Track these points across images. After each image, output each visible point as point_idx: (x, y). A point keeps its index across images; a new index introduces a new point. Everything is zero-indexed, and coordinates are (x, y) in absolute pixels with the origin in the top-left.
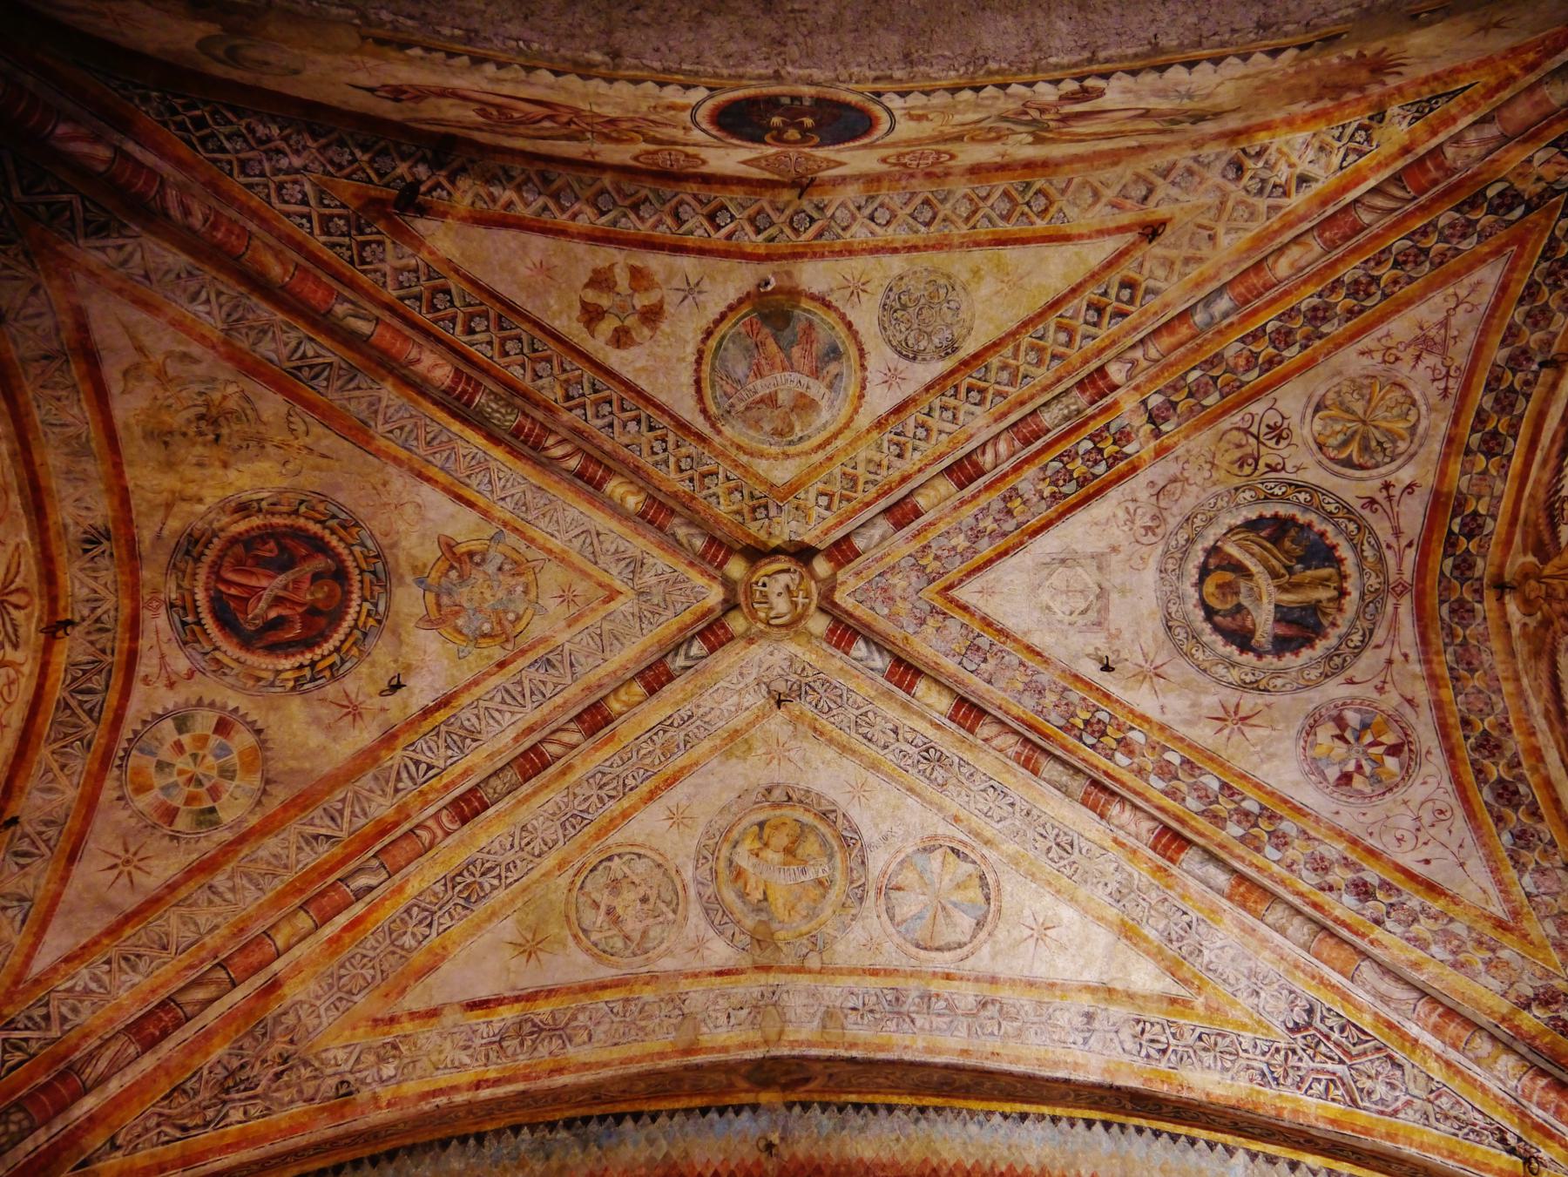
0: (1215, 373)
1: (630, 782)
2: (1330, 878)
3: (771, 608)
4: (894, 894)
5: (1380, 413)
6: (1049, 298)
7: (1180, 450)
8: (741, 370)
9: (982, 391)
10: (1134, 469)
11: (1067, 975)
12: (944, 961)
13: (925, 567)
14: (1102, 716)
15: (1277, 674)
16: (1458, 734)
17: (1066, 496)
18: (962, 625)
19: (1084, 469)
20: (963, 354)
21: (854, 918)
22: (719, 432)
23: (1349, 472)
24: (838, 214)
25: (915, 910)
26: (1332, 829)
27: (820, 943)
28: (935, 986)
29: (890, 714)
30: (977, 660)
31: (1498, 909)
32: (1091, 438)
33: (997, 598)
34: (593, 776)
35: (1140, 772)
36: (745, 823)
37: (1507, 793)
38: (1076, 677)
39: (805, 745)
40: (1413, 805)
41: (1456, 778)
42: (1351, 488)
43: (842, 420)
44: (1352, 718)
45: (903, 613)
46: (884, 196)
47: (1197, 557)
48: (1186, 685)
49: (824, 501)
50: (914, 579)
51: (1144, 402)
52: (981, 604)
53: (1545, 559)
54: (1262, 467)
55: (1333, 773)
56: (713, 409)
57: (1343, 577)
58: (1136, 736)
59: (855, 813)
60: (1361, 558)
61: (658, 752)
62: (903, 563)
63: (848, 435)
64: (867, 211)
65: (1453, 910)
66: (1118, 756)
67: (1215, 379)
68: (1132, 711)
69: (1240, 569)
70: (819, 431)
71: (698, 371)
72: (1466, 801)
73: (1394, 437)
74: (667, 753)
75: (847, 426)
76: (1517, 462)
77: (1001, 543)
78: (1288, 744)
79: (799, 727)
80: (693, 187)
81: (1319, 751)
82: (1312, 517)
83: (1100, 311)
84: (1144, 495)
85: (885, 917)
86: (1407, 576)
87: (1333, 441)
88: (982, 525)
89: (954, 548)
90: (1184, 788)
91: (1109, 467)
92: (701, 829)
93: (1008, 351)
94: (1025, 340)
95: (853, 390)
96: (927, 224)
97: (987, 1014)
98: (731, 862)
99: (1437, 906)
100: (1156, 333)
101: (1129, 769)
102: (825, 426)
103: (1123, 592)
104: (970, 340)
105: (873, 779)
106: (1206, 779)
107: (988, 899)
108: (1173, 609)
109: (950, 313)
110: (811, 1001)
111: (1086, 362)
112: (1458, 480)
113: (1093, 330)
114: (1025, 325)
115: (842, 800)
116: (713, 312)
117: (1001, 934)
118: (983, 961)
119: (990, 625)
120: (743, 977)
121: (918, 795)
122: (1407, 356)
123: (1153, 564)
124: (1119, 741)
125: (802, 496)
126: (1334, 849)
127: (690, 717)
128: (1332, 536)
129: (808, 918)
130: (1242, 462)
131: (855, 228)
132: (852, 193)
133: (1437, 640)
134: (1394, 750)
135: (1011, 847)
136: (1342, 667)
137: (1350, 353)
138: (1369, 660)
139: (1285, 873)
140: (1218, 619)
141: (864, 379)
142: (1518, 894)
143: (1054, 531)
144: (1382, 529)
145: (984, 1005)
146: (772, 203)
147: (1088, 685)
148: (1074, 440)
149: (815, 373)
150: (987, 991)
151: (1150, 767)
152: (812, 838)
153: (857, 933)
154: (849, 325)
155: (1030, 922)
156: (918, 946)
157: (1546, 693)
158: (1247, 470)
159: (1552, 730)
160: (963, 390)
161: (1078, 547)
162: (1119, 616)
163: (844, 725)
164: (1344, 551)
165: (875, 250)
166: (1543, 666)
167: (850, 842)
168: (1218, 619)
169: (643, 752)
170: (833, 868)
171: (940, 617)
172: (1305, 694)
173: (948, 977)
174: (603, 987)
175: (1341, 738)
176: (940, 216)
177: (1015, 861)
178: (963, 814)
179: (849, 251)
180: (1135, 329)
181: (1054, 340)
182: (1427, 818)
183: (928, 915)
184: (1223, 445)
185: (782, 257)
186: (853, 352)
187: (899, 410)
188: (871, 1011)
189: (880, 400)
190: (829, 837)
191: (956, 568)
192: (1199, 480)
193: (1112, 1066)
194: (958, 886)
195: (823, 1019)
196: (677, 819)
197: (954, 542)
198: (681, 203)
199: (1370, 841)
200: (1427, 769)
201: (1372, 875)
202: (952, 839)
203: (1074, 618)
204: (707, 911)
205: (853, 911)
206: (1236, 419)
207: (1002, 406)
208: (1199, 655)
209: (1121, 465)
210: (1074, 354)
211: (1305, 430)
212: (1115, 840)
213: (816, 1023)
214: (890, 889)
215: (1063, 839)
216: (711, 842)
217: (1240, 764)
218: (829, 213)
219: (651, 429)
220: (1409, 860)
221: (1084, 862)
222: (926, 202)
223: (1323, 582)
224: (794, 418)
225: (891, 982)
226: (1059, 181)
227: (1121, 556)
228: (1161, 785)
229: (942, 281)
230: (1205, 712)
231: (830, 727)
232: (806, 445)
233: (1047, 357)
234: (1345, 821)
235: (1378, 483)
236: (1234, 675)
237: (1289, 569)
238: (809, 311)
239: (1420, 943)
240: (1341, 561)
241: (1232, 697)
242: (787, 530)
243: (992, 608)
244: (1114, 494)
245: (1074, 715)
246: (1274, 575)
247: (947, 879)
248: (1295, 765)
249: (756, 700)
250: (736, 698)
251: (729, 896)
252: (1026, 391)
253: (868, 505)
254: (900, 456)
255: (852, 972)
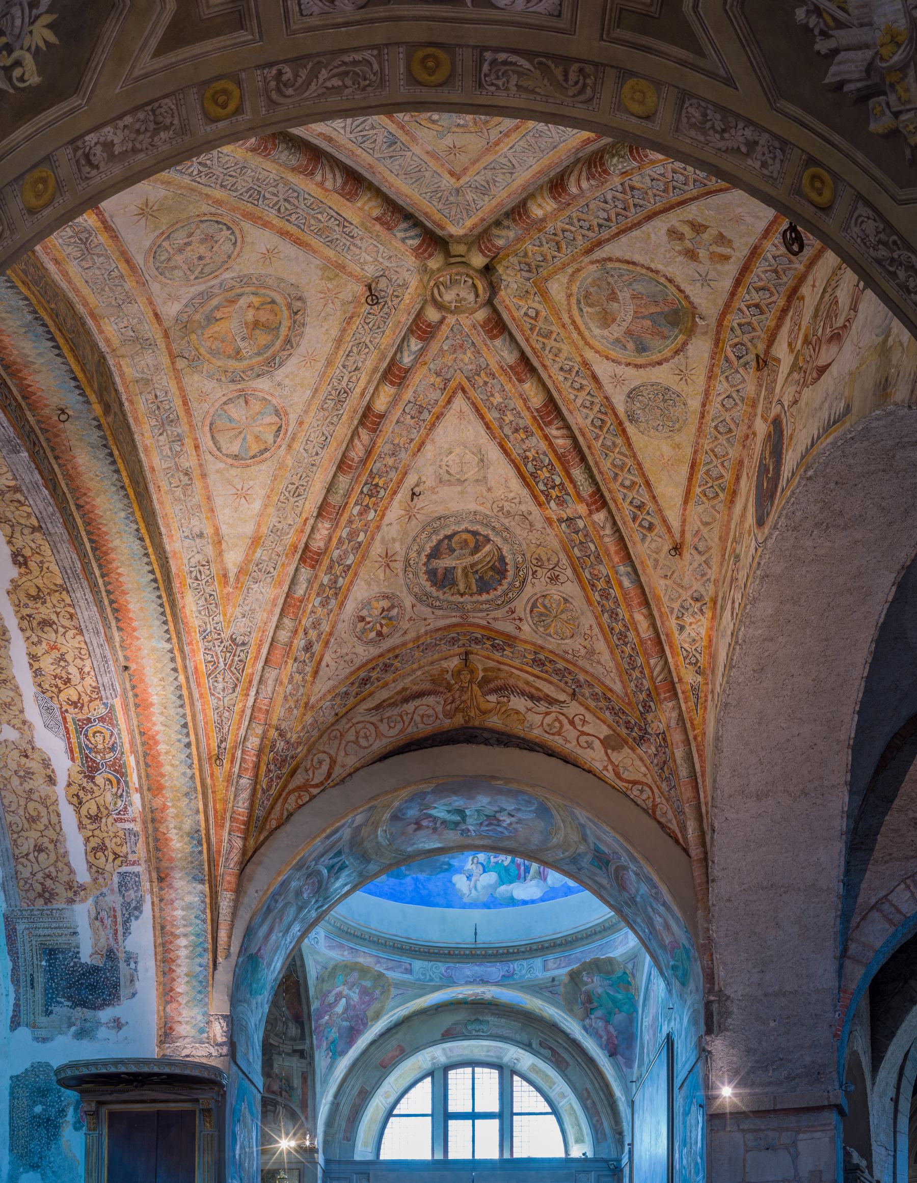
0: (592, 557)
1: (294, 217)
2: (311, 631)
3: (446, 287)
4: (242, 400)
5: (559, 624)
6: (652, 482)
7: (549, 530)
8: (639, 287)
9: (601, 428)
10: (540, 505)
11: (221, 517)
12: (206, 442)
13: (479, 375)
14: (382, 492)
15: (416, 575)
16: (391, 655)
17: (526, 465)
18: (437, 401)
19: (543, 477)
20: (627, 424)
21: (219, 380)
22: (592, 263)
23: (530, 606)
24: (739, 376)
25: (235, 416)
26: (335, 622)
27: (195, 364)
28: (188, 442)
29: (368, 363)
30: (413, 412)
31: (313, 700)
32: (562, 484)
33: (456, 421)
34: (294, 191)
35: (350, 522)
36: (273, 294)
37: (365, 681)
38: (405, 474)
39: (338, 313)
40: (354, 650)
41: (370, 661)
42: (521, 605)
43: (592, 342)
44: (395, 612)
45: (445, 360)
46: (742, 407)
47: (484, 531)
48: (406, 533)
49: (532, 313)
50: (470, 367)
51: (580, 517)
52: (452, 411)
53: (480, 686)
54: (535, 568)
55: (364, 613)
56: (610, 265)
57: (471, 595)
58: (371, 515)
59: (294, 360)
60: (482, 603)
61: (321, 225)
62: (482, 359)
63: (581, 343)
64: (734, 395)
65: (308, 685)
66: (358, 508)
67: (588, 556)
68: (386, 508)
69: (476, 550)
70: (586, 324)
71: (642, 266)
72: (359, 669)
73: (547, 627)
74: (320, 232)
75: (587, 343)
76: (530, 669)
77: (495, 425)
78: (376, 590)
79: (352, 305)
80: (782, 302)
81: (375, 604)
82: (505, 586)
83: (639, 508)
84: (523, 508)
85: (225, 399)
86: (471, 620)
87: (546, 602)
88: (508, 413)
89: (492, 395)
90: (344, 547)
91: (542, 492)
92: (263, 272)
93: (624, 450)
94: (630, 462)
95: (613, 354)
96: (716, 427)
97: (182, 478)
98: (241, 295)
99: (309, 678)
100: (621, 540)
101: (351, 514)
102: (589, 329)
103: (462, 493)
104: (636, 431)
105: (319, 366)
106: (351, 557)
107: (253, 457)
108: (452, 519)
109: (655, 425)
110: (152, 368)
111: (610, 492)
112: (521, 647)
113: (629, 500)
114: (639, 464)
115: (301, 350)
116: (688, 290)
117: (234, 472)
118: (214, 466)
119: (438, 418)
120: (157, 326)
121: (313, 396)
122: (586, 643)
123: (480, 508)
124: (367, 506)
125: (537, 299)
126: (325, 627)
127: (352, 237)
128: (493, 595)
129: (211, 351)
130: (539, 559)
131: (725, 384)
132: (750, 388)
133: (438, 635)
134: (380, 634)
135: (289, 461)
136: (421, 601)
137: (593, 622)
138: (426, 611)
139: (308, 611)
140: (446, 541)
141: (619, 363)
142: (320, 704)
143: (502, 457)
144: (499, 613)
145: (186, 474)
146: (759, 337)
147: (401, 482)
148: (562, 474)
149: (629, 333)
150: (196, 473)
151: (354, 526)
152: (269, 338)
153: (209, 385)
154: (660, 363)
155: (246, 486)
156: (211, 424)
157: (415, 688)
158: (534, 562)
159: (397, 693)
160: (603, 417)
161: (491, 469)
162: (445, 492)
163: (358, 336)
164: (485, 597)
165: (707, 393)
166: (427, 686)
167: (272, 363)
168: (446, 541)
169: (319, 216)
170: (251, 358)
171: (442, 386)
172: (405, 589)
173: (197, 447)
174: (128, 261)
175: (383, 610)
176: (719, 436)
177: (282, 466)
178: (305, 426)
179: (710, 377)
180: (625, 523)
181: (627, 479)
182: (347, 658)
183: (233, 425)
184: (550, 553)
185: (718, 333)
186: (640, 361)
187: (595, 378)
188: (158, 408)
189: (603, 369)
190: (273, 349)
191: (478, 396)
192: (530, 537)
193: (178, 555)
194: (257, 437)
195: (142, 379)
196: (269, 255)
197: (497, 395)
198: (772, 294)
199: (332, 640)
200: (372, 650)
201: (317, 648)
202: (287, 425)
203: (445, 468)
204: (202, 293)
205: (223, 379)
206: (564, 561)
207: (589, 436)
208: (424, 535)
209: (543, 498)
210: (615, 486)
211: (554, 591)
212: (307, 519)
213: (139, 376)
214: (245, 397)
215: (301, 489)
216: (254, 280)
217: (362, 572)
218: (740, 370)
219: (600, 226)
220: (327, 658)
221: (290, 506)
222: (730, 431)
223: (468, 586)
224: (598, 309)
225: (182, 414)
226: (721, 507)
227: (485, 493)
228: (344, 535)
229: (677, 426)
230: (390, 546)
231: (354, 327)
232: (575, 313)
233: (617, 471)
234: (340, 626)
235: (523, 616)
236: (413, 555)
237: (477, 572)
238: (675, 339)
239: (290, 682)
240: (480, 594)
241: (400, 557)
242: (509, 279)
243: (450, 419)
244: (525, 492)
245: (380, 477)
246: (472, 566)
247: (260, 429)
248: (366, 595)
249: (370, 271)
250: (370, 259)
251: (215, 302)
252: (597, 453)
253: (527, 340)
254: (561, 369)
255: (181, 389)
